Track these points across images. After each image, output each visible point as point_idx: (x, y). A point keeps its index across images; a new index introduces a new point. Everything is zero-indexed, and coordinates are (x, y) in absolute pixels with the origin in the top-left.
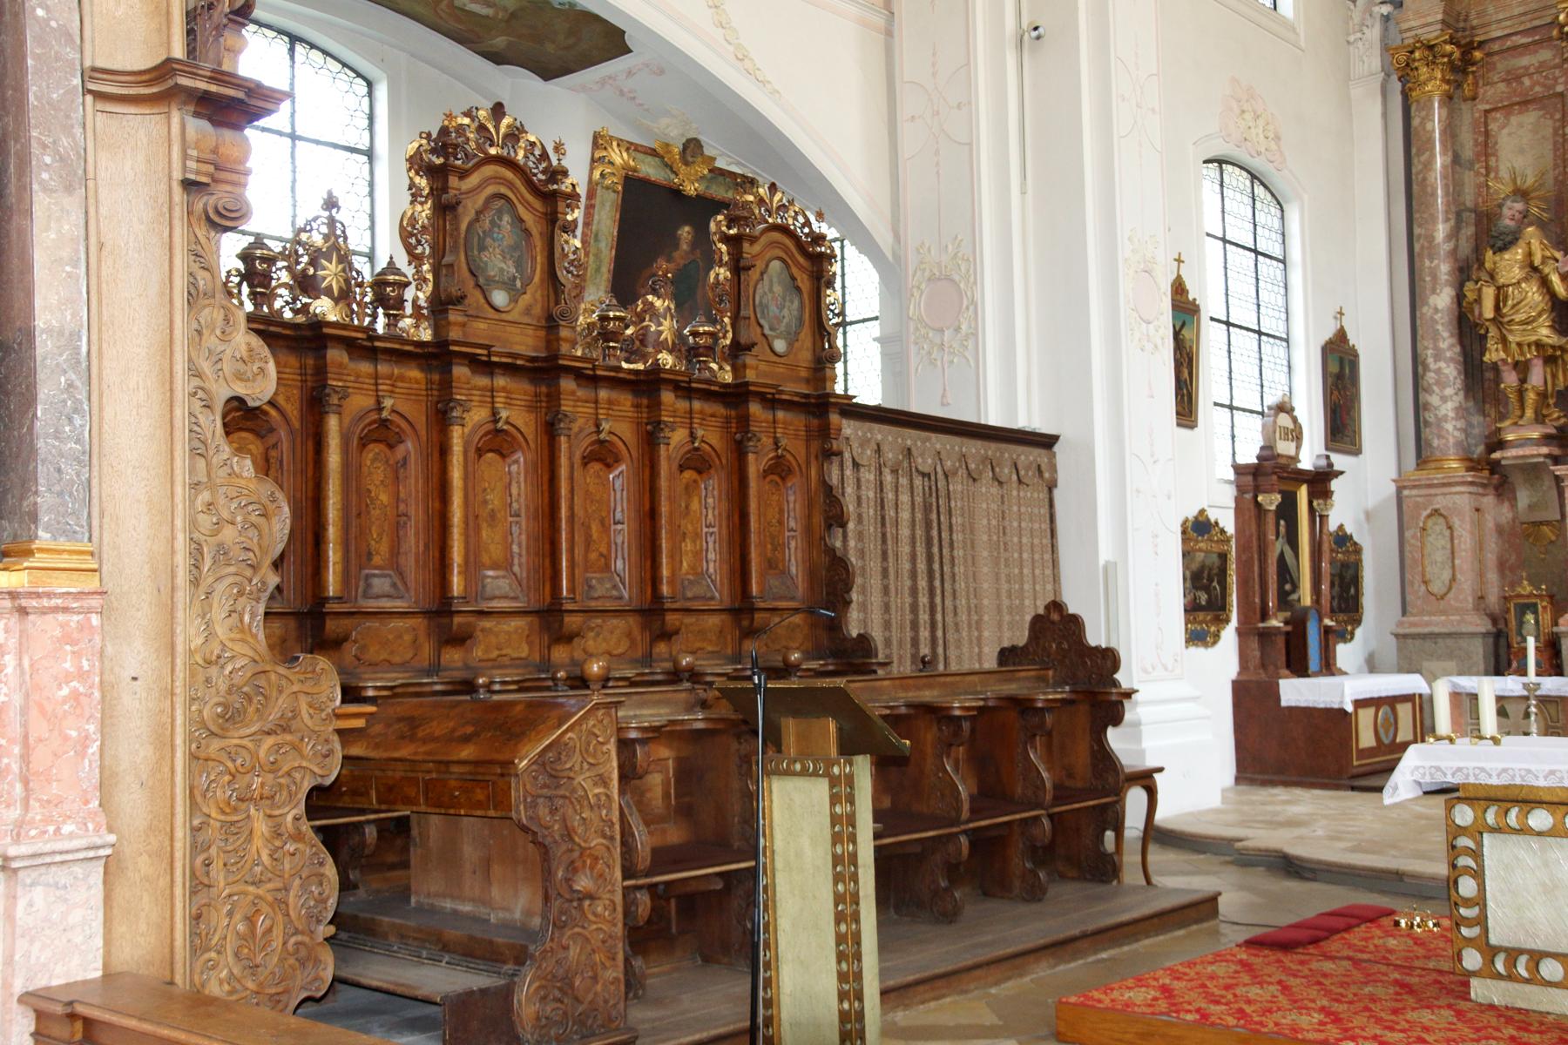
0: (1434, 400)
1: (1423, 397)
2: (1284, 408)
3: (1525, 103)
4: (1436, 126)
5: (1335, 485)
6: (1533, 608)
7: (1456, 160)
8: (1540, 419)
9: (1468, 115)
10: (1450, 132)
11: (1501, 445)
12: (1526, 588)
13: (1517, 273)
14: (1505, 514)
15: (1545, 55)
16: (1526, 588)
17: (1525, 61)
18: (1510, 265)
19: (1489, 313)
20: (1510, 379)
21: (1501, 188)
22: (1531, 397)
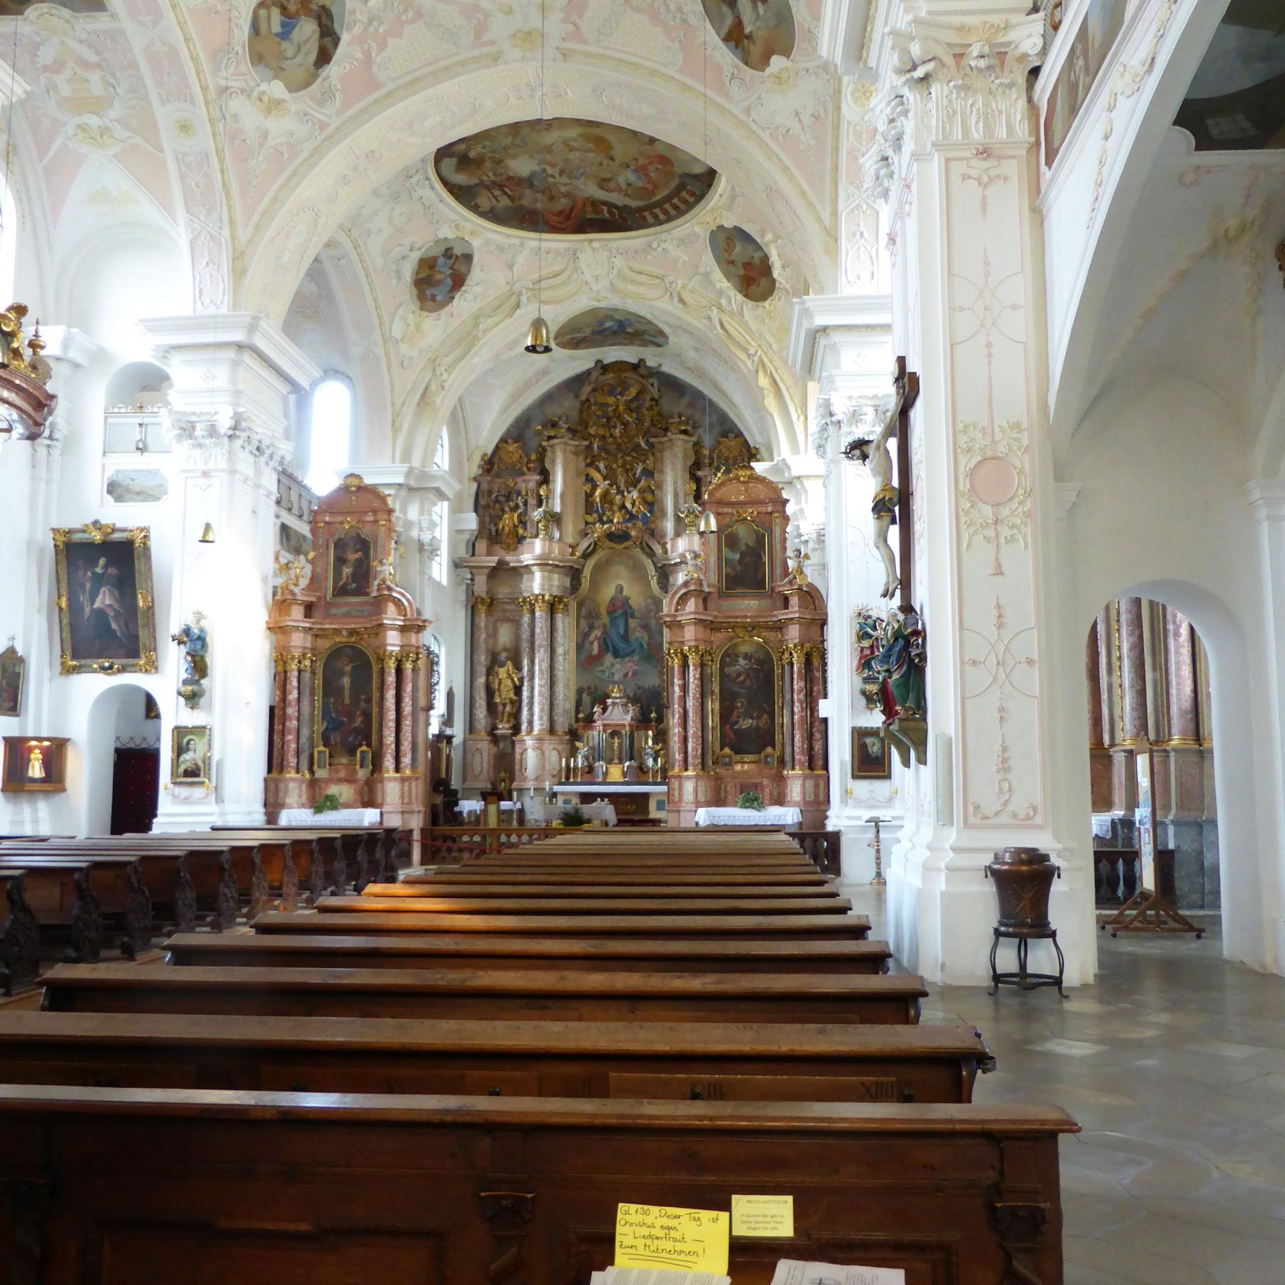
0: (478, 712)
1: (475, 711)
2: (443, 715)
3: (508, 620)
4: (482, 624)
5: (454, 740)
6: (504, 781)
7: (488, 636)
8: (508, 722)
9: (491, 620)
10: (486, 627)
11: (496, 728)
12: (503, 774)
13: (505, 675)
14: (494, 750)
15: (512, 607)
16: (503, 774)
17: (508, 607)
18: (502, 672)
19: (497, 687)
20: (500, 708)
21: (499, 647)
22: (506, 714)
